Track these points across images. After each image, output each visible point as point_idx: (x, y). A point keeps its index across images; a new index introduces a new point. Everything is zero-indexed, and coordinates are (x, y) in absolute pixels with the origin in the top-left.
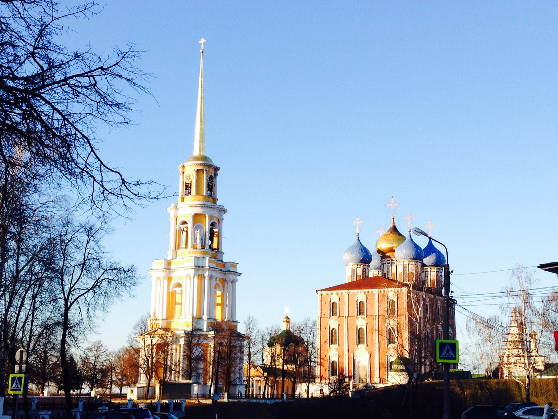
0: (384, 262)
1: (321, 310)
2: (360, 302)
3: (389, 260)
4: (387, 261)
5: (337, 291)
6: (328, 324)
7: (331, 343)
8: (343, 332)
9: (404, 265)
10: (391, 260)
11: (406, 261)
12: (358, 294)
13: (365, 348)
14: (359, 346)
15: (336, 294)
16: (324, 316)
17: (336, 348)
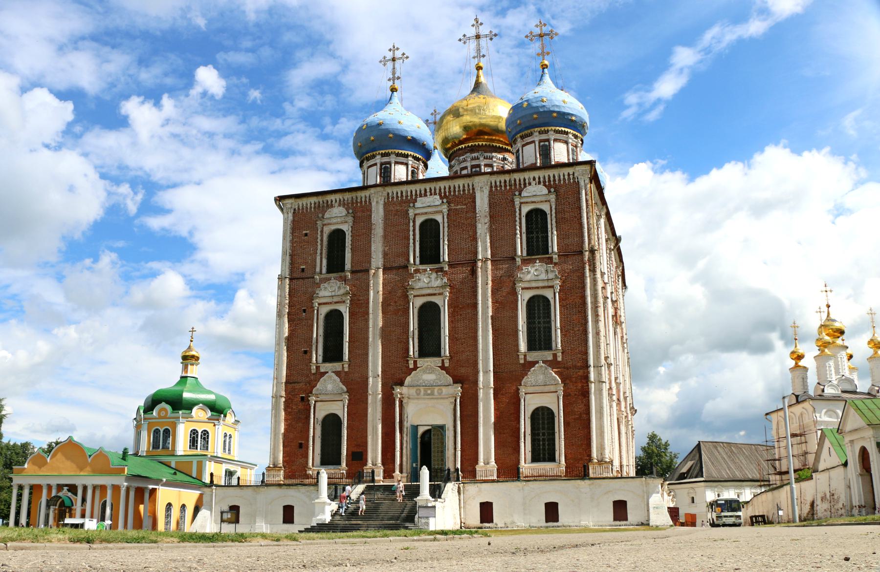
0: (463, 165)
1: (291, 256)
2: (423, 225)
3: (478, 159)
4: (473, 159)
5: (347, 196)
6: (311, 299)
7: (320, 359)
8: (367, 321)
9: (542, 144)
10: (482, 159)
11: (547, 132)
12: (418, 199)
13: (443, 367)
14: (421, 362)
15: (342, 203)
16: (304, 275)
17: (338, 373)
